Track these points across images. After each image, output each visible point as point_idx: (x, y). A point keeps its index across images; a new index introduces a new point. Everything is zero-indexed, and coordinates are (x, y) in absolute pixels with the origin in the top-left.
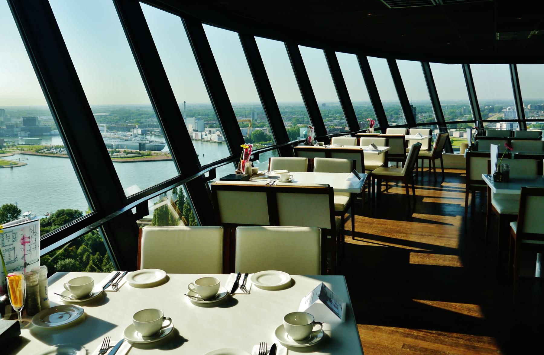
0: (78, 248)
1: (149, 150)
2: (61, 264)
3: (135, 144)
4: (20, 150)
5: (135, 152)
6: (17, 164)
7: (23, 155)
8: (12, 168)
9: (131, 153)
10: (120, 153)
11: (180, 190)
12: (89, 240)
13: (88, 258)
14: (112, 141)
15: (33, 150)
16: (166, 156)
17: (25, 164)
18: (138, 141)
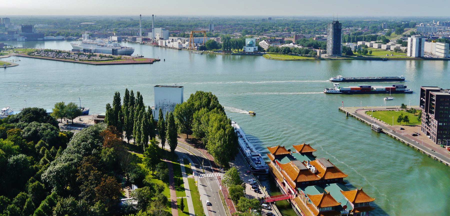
0: (36, 143)
1: (120, 55)
2: (13, 159)
3: (109, 50)
4: (15, 53)
5: (108, 56)
6: (10, 65)
7: (17, 57)
8: (5, 68)
9: (105, 57)
10: (96, 57)
11: (131, 93)
12: (47, 135)
13: (43, 151)
14: (91, 46)
15: (26, 53)
16: (133, 60)
17: (17, 65)
18: (112, 47)
